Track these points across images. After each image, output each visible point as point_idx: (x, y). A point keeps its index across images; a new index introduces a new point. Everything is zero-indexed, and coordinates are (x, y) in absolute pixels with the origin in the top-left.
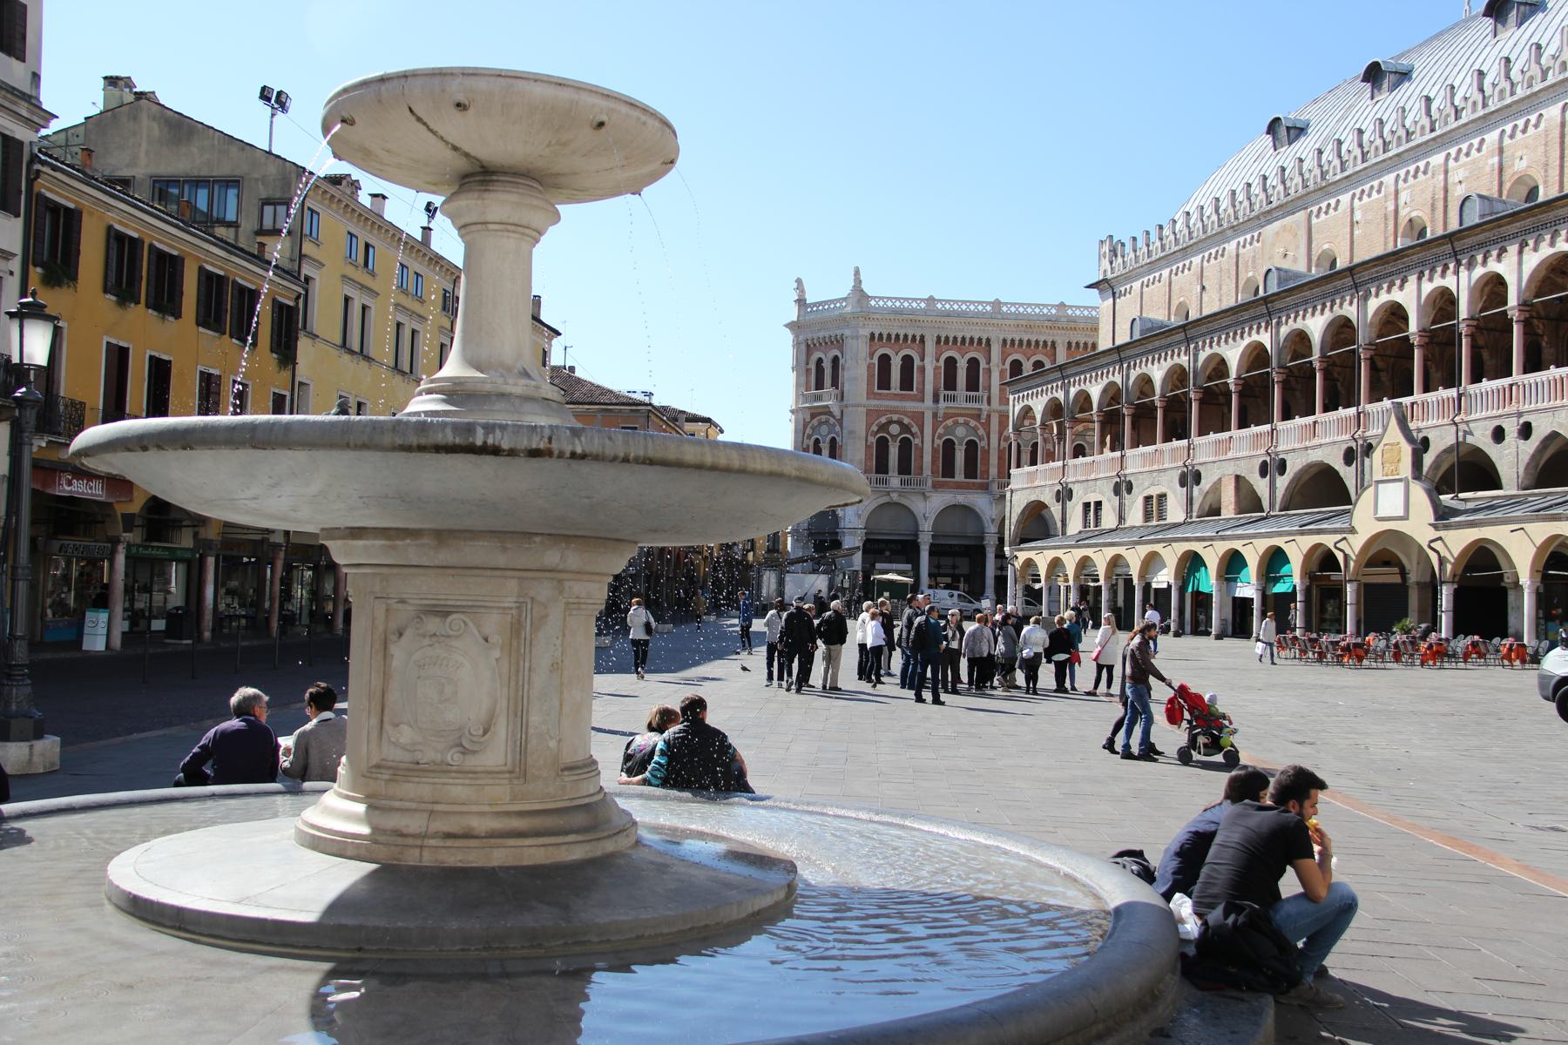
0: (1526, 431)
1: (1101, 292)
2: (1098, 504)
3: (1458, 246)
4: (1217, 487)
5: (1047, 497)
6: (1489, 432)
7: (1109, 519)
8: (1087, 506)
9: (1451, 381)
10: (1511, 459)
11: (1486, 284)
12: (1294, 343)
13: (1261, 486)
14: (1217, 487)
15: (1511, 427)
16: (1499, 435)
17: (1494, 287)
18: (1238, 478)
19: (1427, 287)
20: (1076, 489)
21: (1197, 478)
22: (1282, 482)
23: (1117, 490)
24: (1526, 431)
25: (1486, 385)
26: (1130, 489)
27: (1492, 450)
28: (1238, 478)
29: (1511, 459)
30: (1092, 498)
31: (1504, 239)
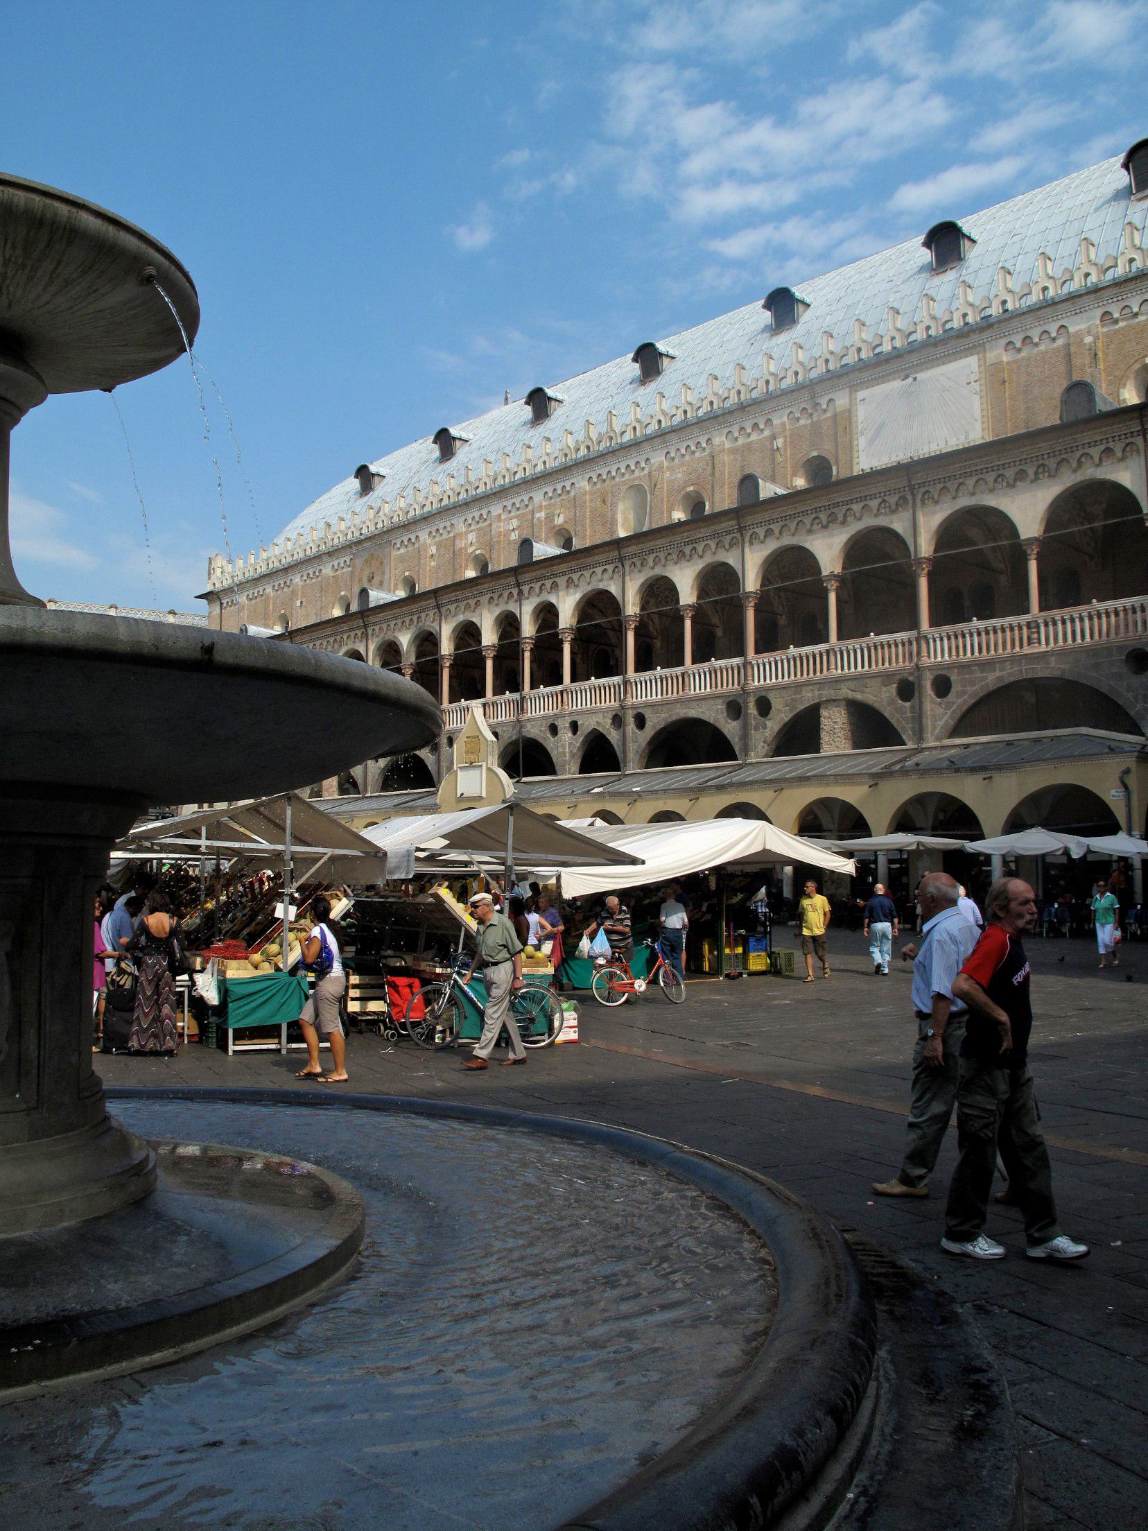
1: (210, 602)
3: (522, 578)
9: (516, 686)
11: (541, 611)
12: (385, 651)
17: (547, 614)
19: (497, 611)
25: (542, 689)
31: (556, 575)
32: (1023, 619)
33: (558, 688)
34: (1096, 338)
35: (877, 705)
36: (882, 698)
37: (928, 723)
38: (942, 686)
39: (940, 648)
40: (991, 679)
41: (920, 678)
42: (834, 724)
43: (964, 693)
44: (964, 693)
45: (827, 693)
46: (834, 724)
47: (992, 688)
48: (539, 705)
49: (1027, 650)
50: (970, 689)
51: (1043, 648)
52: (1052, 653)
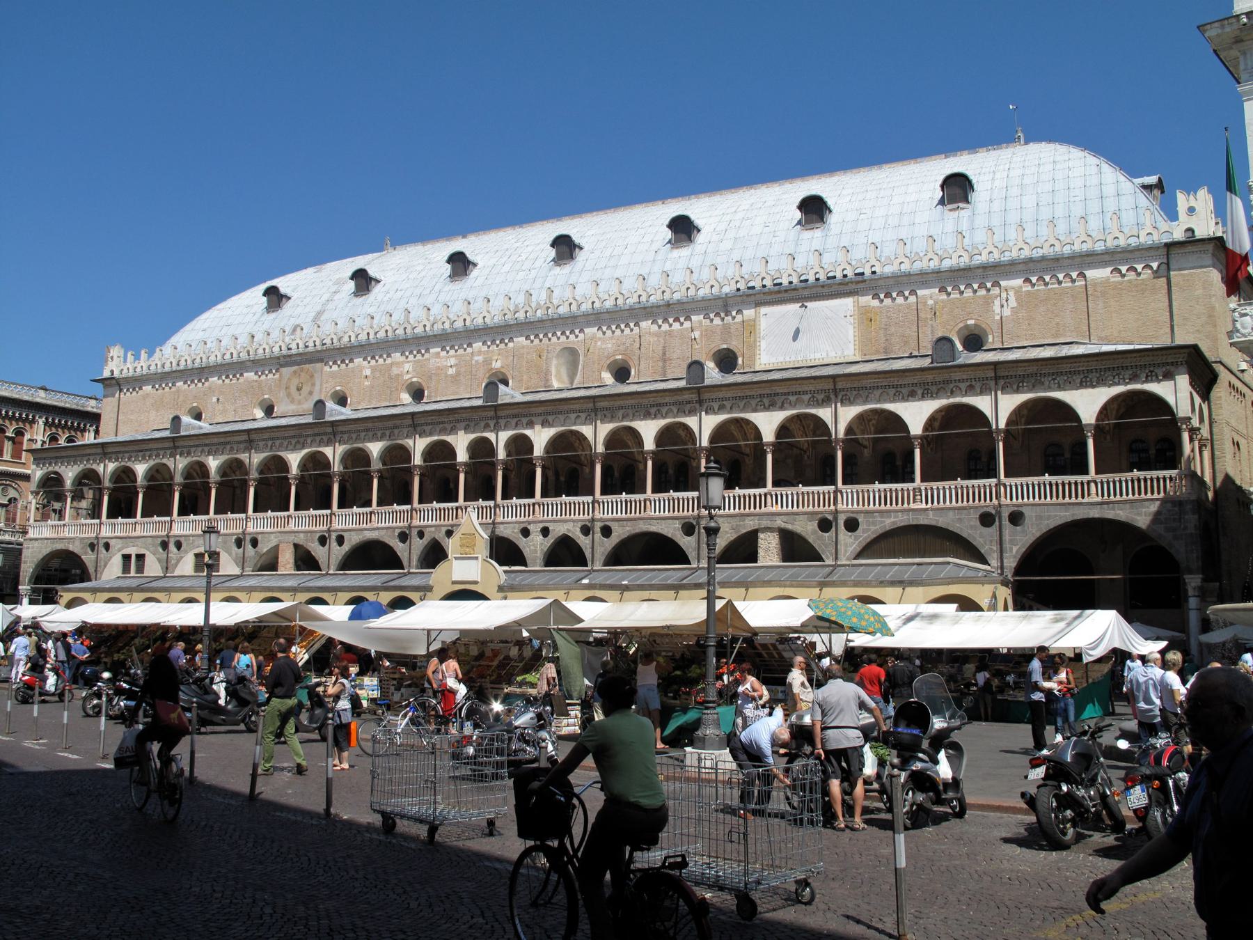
0: (545, 532)
2: (140, 557)
4: (276, 550)
5: (75, 548)
6: (517, 529)
7: (153, 567)
8: (127, 558)
9: (490, 495)
10: (535, 547)
13: (319, 552)
14: (276, 550)
15: (535, 529)
16: (525, 532)
18: (296, 546)
20: (112, 542)
21: (255, 543)
22: (338, 552)
23: (165, 545)
24: (545, 532)
26: (179, 545)
27: (522, 542)
28: (296, 546)
29: (535, 547)
30: (133, 551)
32: (910, 486)
33: (531, 501)
34: (936, 303)
35: (803, 534)
36: (807, 529)
37: (841, 548)
38: (852, 525)
39: (850, 498)
40: (889, 523)
41: (836, 519)
42: (769, 548)
43: (868, 530)
44: (868, 530)
45: (765, 523)
46: (769, 548)
47: (888, 528)
48: (511, 515)
49: (913, 506)
50: (873, 528)
51: (923, 506)
52: (932, 509)
